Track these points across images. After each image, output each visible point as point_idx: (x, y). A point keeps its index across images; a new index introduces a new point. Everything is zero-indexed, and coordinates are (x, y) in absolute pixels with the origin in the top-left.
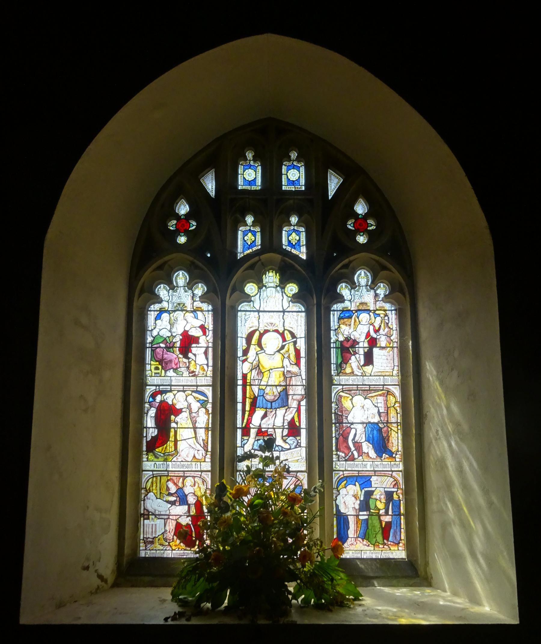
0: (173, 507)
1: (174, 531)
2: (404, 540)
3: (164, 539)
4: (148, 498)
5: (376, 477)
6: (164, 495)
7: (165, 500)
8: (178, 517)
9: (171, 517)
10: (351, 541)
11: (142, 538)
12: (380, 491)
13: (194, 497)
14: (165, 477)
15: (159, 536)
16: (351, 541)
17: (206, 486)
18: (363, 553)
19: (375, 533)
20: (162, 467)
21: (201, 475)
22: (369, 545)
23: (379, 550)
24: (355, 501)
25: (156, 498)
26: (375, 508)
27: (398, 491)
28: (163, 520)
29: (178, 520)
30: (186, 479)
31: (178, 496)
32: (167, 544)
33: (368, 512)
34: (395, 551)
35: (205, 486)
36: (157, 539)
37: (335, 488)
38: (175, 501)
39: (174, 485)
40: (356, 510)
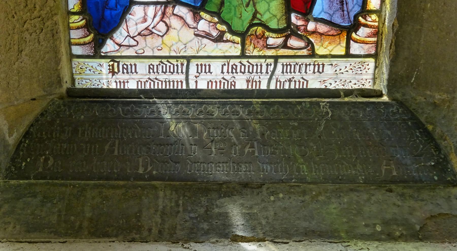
10: (145, 20)
16: (145, 20)
18: (193, 70)
22: (222, 33)
23: (265, 57)
34: (335, 61)
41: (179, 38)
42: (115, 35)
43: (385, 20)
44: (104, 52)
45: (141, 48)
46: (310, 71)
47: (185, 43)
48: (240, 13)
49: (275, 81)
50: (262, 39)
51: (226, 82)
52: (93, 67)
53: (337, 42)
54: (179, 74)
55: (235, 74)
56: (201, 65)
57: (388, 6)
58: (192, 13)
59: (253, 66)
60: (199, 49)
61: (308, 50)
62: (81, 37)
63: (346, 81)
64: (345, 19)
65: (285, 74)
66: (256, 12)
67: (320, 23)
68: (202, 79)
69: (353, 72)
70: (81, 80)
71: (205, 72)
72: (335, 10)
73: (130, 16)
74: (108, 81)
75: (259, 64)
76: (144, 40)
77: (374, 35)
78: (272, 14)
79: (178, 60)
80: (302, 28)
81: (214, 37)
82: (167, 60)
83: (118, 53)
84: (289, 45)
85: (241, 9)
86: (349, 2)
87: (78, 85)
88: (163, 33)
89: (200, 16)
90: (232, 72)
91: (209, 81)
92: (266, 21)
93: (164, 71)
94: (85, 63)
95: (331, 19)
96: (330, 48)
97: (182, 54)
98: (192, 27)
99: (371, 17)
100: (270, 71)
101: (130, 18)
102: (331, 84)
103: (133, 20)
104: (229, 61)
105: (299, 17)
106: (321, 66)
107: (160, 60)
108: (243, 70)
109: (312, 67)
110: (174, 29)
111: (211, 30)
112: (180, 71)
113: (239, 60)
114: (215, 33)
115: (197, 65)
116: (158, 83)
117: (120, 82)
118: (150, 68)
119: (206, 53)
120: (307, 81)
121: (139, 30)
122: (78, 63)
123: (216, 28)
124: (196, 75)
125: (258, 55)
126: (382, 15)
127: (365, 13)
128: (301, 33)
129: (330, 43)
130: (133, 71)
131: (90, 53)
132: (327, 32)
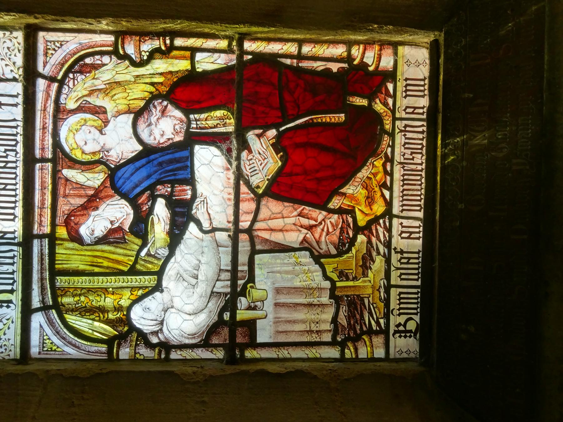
0: (199, 211)
1: (307, 209)
3: (340, 254)
4: (156, 329)
6: (143, 253)
7: (166, 252)
8: (244, 188)
9: (244, 224)
11: (333, 353)
13: (156, 112)
14: (59, 250)
15: (326, 277)
17: (102, 53)
20: (10, 268)
21: (51, 79)
25: (157, 294)
28: (257, 257)
29: (260, 191)
30: (67, 149)
31: (152, 188)
32: (361, 238)
35: (106, 59)
36: (339, 284)
38: (172, 203)
39: (97, 208)
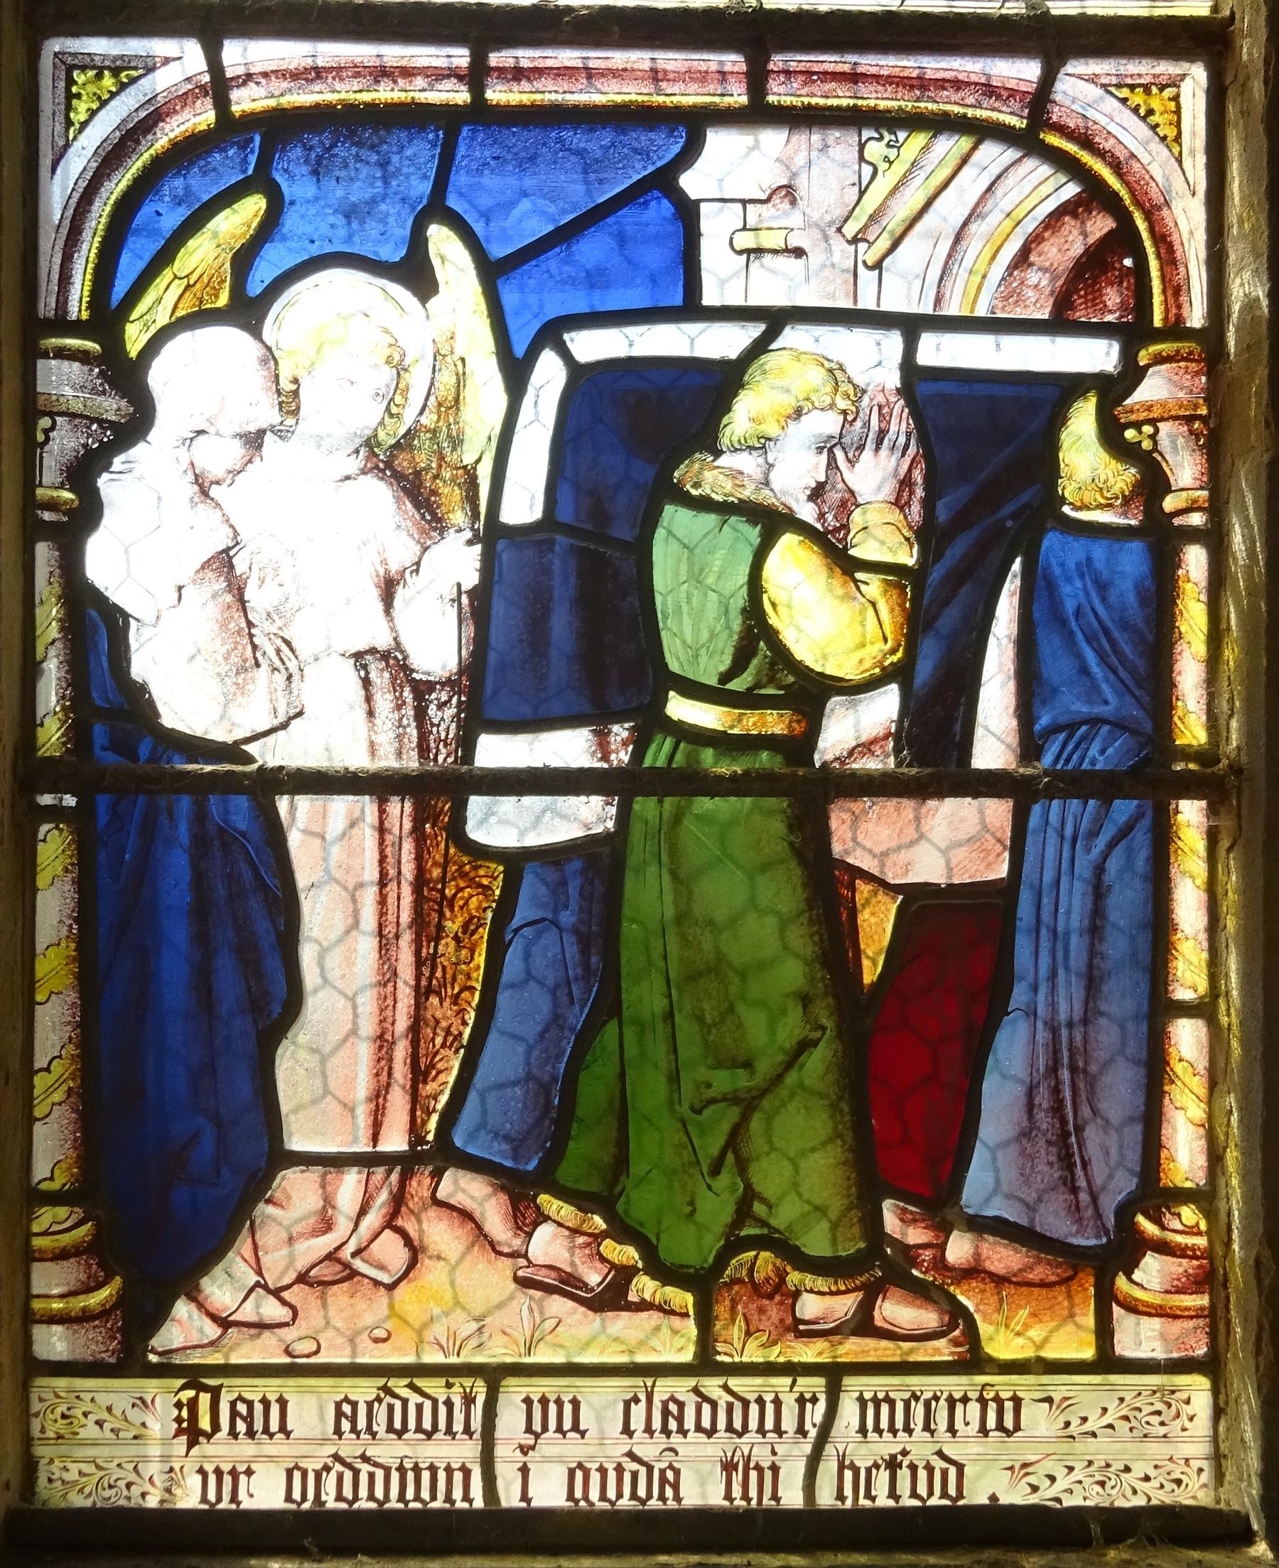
2: (1205, 1198)
5: (773, 139)
10: (326, 1225)
12: (836, 372)
18: (511, 1420)
19: (723, 1081)
22: (624, 1275)
23: (793, 1370)
24: (402, 550)
26: (739, 665)
27: (1131, 374)
33: (620, 732)
34: (1060, 1385)
37: (63, 325)
40: (422, 690)
41: (455, 1297)
42: (205, 1282)
43: (1229, 1230)
44: (160, 1349)
45: (310, 1333)
46: (967, 1424)
47: (478, 1310)
48: (687, 1199)
49: (834, 1465)
50: (778, 1298)
51: (643, 1471)
52: (114, 1411)
53: (1063, 1308)
54: (454, 1439)
55: (676, 1439)
56: (544, 1401)
57: (1235, 1182)
58: (506, 1197)
59: (746, 1404)
60: (533, 1336)
61: (956, 1343)
62: (73, 1289)
63: (1108, 1466)
64: (1085, 1223)
65: (872, 1436)
66: (747, 1200)
67: (991, 1239)
68: (547, 1460)
69: (1131, 1429)
70: (62, 1465)
71: (559, 1429)
72: (1042, 1187)
73: (270, 1209)
74: (171, 1470)
75: (768, 1398)
76: (319, 1301)
77: (1196, 1283)
78: (809, 1202)
79: (451, 1380)
80: (927, 1255)
81: (592, 1290)
82: (406, 1381)
83: (217, 1355)
84: (879, 1322)
85: (690, 1184)
86: (1093, 1159)
87: (49, 1486)
88: (392, 1276)
89: (538, 1208)
90: (666, 1431)
91: (574, 1465)
92: (789, 1228)
93: (398, 1424)
94: (82, 1395)
95: (1032, 1220)
96: (1036, 1333)
97: (470, 1356)
98: (506, 1250)
99: (1179, 1215)
100: (814, 1425)
101: (269, 1216)
102: (1052, 1479)
103: (280, 1224)
104: (653, 1386)
105: (911, 1212)
106: (1009, 1405)
107: (381, 1382)
108: (706, 1423)
109: (974, 1408)
110: (439, 1258)
111: (577, 1261)
112: (458, 1427)
113: (692, 1382)
114: (594, 1277)
115: (528, 1401)
116: (371, 1476)
117: (219, 1473)
118: (339, 1414)
119: (561, 1352)
120: (960, 1468)
121: (301, 1264)
122: (52, 1396)
123: (599, 1253)
124: (523, 1442)
125: (761, 1360)
126: (1218, 1210)
127: (1154, 1202)
128: (921, 1276)
129: (1034, 1315)
130: (274, 1425)
131: (103, 1355)
132: (1020, 1270)
